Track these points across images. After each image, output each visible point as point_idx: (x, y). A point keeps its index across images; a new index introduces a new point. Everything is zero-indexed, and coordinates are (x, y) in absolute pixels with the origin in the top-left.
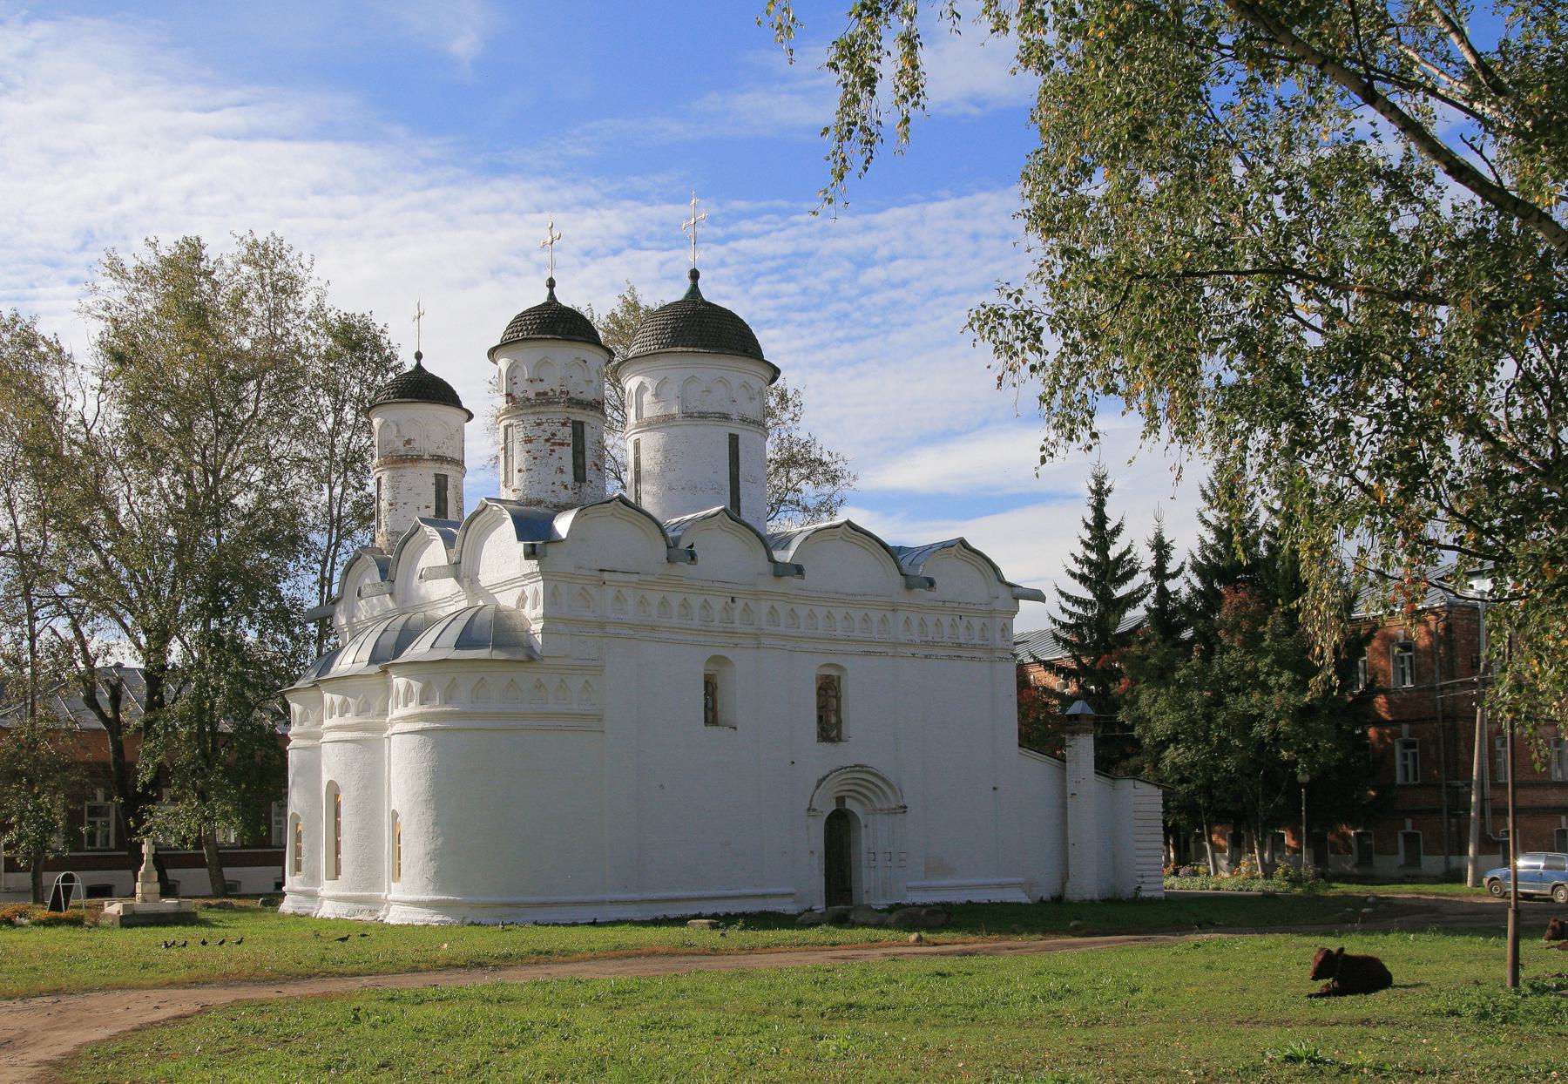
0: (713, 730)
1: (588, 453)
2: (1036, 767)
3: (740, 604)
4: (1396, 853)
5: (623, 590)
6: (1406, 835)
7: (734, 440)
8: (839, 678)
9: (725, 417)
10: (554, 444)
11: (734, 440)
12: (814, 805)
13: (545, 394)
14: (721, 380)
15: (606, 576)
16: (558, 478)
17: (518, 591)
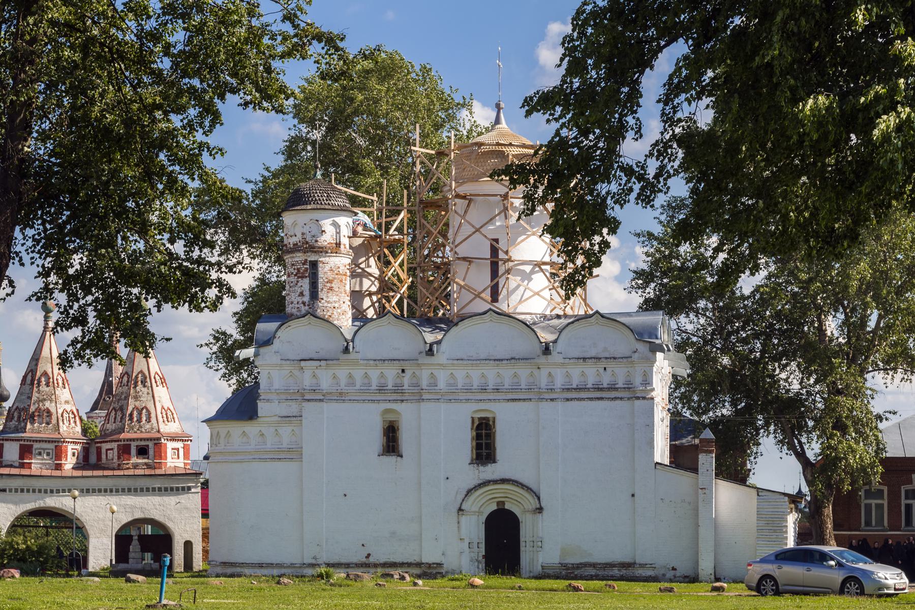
0: (392, 459)
3: (408, 373)
5: (317, 371)
8: (494, 418)
10: (299, 277)
12: (463, 507)
13: (297, 244)
15: (303, 363)
16: (300, 299)
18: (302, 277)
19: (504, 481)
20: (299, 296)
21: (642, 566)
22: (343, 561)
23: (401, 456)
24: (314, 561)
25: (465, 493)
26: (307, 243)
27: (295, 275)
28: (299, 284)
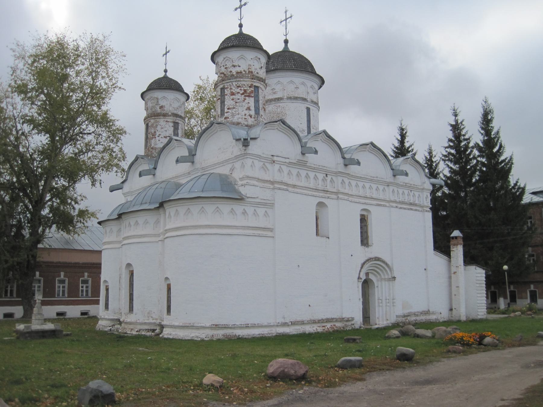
1: (261, 102)
2: (439, 260)
4: (527, 298)
6: (531, 292)
7: (308, 109)
9: (305, 100)
10: (245, 96)
11: (308, 109)
13: (241, 72)
14: (303, 84)
16: (247, 112)
17: (230, 166)
18: (249, 96)
19: (377, 259)
20: (246, 110)
21: (433, 313)
22: (299, 319)
23: (328, 238)
24: (283, 321)
25: (360, 266)
26: (252, 72)
27: (242, 94)
28: (246, 101)
